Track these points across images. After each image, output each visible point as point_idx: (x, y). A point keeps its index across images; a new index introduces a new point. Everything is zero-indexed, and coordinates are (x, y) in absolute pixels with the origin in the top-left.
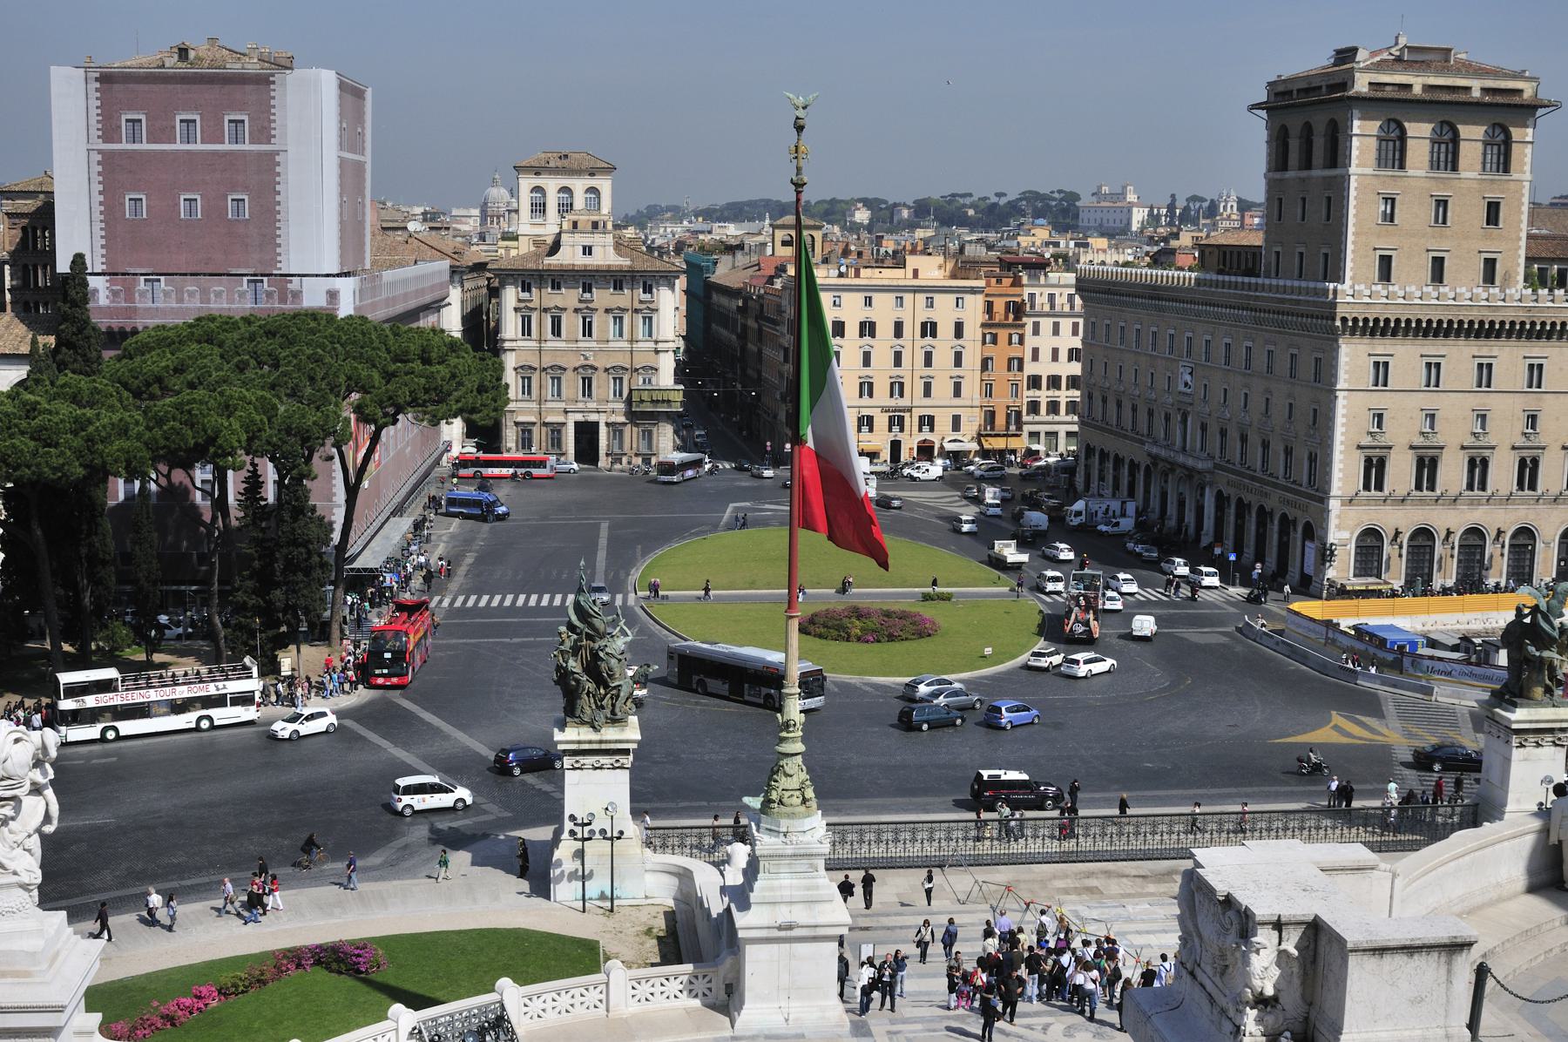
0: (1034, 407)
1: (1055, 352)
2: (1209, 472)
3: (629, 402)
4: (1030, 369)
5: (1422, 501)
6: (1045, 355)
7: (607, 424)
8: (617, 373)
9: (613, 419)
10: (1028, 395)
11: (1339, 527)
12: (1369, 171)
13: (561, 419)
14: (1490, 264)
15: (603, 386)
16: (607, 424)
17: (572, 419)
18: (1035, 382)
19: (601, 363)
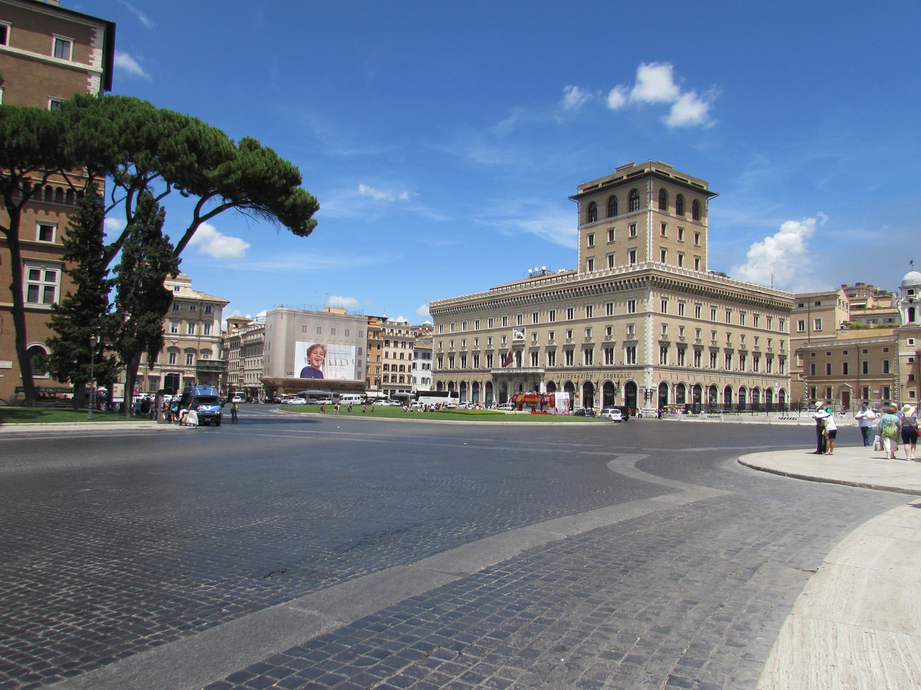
0: (386, 377)
1: (395, 354)
2: (544, 374)
3: (197, 367)
4: (385, 361)
5: (681, 369)
6: (391, 355)
7: (184, 378)
8: (190, 351)
9: (186, 376)
10: (382, 373)
11: (653, 380)
12: (657, 210)
13: (158, 374)
14: (697, 261)
15: (181, 359)
16: (184, 378)
17: (163, 375)
18: (386, 367)
19: (182, 346)
